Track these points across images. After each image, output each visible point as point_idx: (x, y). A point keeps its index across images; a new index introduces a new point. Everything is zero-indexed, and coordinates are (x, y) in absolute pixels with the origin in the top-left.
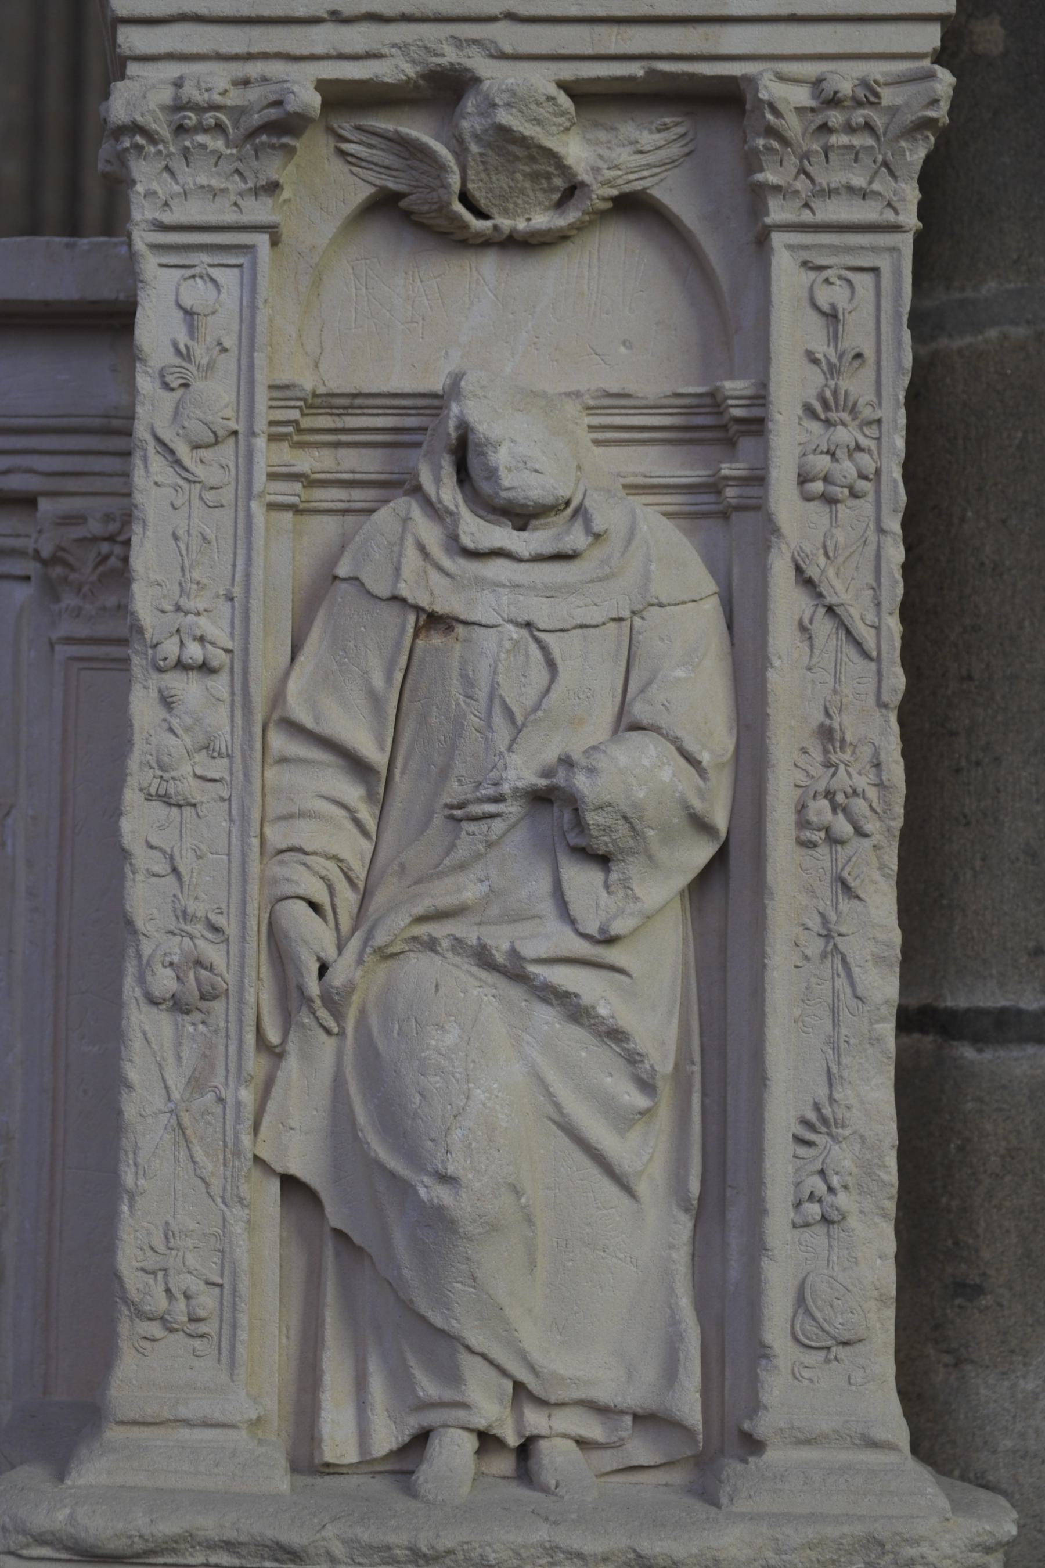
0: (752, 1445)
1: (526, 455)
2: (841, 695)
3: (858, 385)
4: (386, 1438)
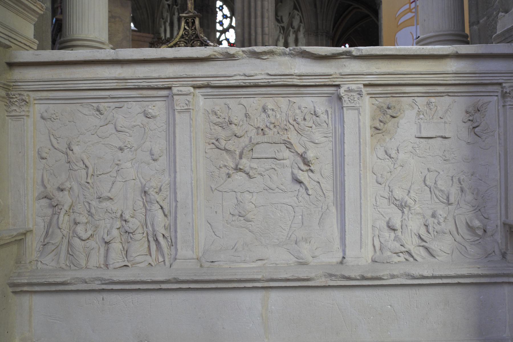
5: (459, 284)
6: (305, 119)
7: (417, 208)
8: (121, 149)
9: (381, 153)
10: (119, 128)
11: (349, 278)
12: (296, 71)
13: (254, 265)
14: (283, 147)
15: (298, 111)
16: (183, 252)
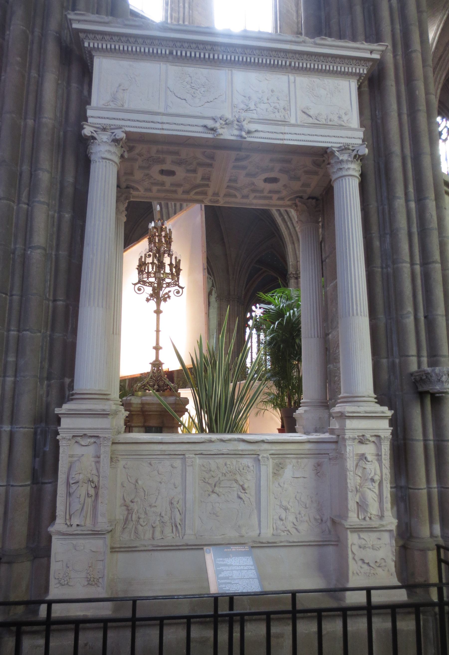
0: (383, 517)
1: (369, 458)
2: (387, 472)
3: (387, 453)
4: (363, 518)
5: (309, 545)
6: (243, 469)
7: (292, 510)
8: (161, 483)
9: (277, 485)
10: (160, 473)
11: (262, 543)
12: (240, 448)
13: (220, 537)
14: (234, 482)
15: (240, 465)
16: (188, 531)
